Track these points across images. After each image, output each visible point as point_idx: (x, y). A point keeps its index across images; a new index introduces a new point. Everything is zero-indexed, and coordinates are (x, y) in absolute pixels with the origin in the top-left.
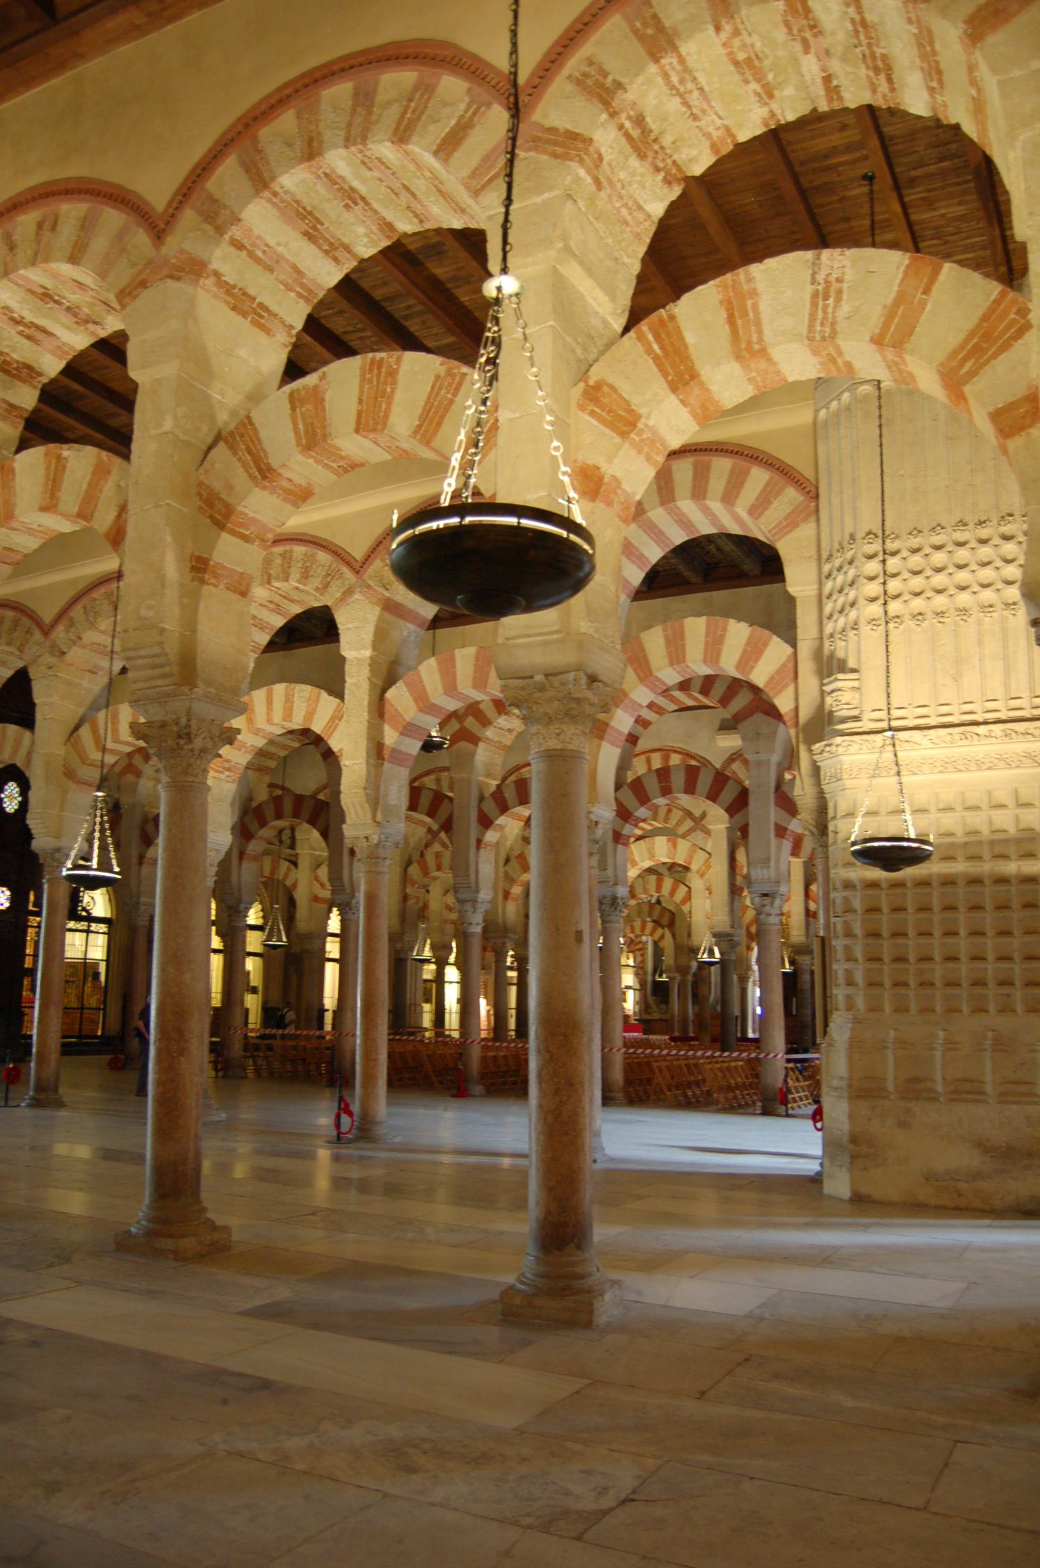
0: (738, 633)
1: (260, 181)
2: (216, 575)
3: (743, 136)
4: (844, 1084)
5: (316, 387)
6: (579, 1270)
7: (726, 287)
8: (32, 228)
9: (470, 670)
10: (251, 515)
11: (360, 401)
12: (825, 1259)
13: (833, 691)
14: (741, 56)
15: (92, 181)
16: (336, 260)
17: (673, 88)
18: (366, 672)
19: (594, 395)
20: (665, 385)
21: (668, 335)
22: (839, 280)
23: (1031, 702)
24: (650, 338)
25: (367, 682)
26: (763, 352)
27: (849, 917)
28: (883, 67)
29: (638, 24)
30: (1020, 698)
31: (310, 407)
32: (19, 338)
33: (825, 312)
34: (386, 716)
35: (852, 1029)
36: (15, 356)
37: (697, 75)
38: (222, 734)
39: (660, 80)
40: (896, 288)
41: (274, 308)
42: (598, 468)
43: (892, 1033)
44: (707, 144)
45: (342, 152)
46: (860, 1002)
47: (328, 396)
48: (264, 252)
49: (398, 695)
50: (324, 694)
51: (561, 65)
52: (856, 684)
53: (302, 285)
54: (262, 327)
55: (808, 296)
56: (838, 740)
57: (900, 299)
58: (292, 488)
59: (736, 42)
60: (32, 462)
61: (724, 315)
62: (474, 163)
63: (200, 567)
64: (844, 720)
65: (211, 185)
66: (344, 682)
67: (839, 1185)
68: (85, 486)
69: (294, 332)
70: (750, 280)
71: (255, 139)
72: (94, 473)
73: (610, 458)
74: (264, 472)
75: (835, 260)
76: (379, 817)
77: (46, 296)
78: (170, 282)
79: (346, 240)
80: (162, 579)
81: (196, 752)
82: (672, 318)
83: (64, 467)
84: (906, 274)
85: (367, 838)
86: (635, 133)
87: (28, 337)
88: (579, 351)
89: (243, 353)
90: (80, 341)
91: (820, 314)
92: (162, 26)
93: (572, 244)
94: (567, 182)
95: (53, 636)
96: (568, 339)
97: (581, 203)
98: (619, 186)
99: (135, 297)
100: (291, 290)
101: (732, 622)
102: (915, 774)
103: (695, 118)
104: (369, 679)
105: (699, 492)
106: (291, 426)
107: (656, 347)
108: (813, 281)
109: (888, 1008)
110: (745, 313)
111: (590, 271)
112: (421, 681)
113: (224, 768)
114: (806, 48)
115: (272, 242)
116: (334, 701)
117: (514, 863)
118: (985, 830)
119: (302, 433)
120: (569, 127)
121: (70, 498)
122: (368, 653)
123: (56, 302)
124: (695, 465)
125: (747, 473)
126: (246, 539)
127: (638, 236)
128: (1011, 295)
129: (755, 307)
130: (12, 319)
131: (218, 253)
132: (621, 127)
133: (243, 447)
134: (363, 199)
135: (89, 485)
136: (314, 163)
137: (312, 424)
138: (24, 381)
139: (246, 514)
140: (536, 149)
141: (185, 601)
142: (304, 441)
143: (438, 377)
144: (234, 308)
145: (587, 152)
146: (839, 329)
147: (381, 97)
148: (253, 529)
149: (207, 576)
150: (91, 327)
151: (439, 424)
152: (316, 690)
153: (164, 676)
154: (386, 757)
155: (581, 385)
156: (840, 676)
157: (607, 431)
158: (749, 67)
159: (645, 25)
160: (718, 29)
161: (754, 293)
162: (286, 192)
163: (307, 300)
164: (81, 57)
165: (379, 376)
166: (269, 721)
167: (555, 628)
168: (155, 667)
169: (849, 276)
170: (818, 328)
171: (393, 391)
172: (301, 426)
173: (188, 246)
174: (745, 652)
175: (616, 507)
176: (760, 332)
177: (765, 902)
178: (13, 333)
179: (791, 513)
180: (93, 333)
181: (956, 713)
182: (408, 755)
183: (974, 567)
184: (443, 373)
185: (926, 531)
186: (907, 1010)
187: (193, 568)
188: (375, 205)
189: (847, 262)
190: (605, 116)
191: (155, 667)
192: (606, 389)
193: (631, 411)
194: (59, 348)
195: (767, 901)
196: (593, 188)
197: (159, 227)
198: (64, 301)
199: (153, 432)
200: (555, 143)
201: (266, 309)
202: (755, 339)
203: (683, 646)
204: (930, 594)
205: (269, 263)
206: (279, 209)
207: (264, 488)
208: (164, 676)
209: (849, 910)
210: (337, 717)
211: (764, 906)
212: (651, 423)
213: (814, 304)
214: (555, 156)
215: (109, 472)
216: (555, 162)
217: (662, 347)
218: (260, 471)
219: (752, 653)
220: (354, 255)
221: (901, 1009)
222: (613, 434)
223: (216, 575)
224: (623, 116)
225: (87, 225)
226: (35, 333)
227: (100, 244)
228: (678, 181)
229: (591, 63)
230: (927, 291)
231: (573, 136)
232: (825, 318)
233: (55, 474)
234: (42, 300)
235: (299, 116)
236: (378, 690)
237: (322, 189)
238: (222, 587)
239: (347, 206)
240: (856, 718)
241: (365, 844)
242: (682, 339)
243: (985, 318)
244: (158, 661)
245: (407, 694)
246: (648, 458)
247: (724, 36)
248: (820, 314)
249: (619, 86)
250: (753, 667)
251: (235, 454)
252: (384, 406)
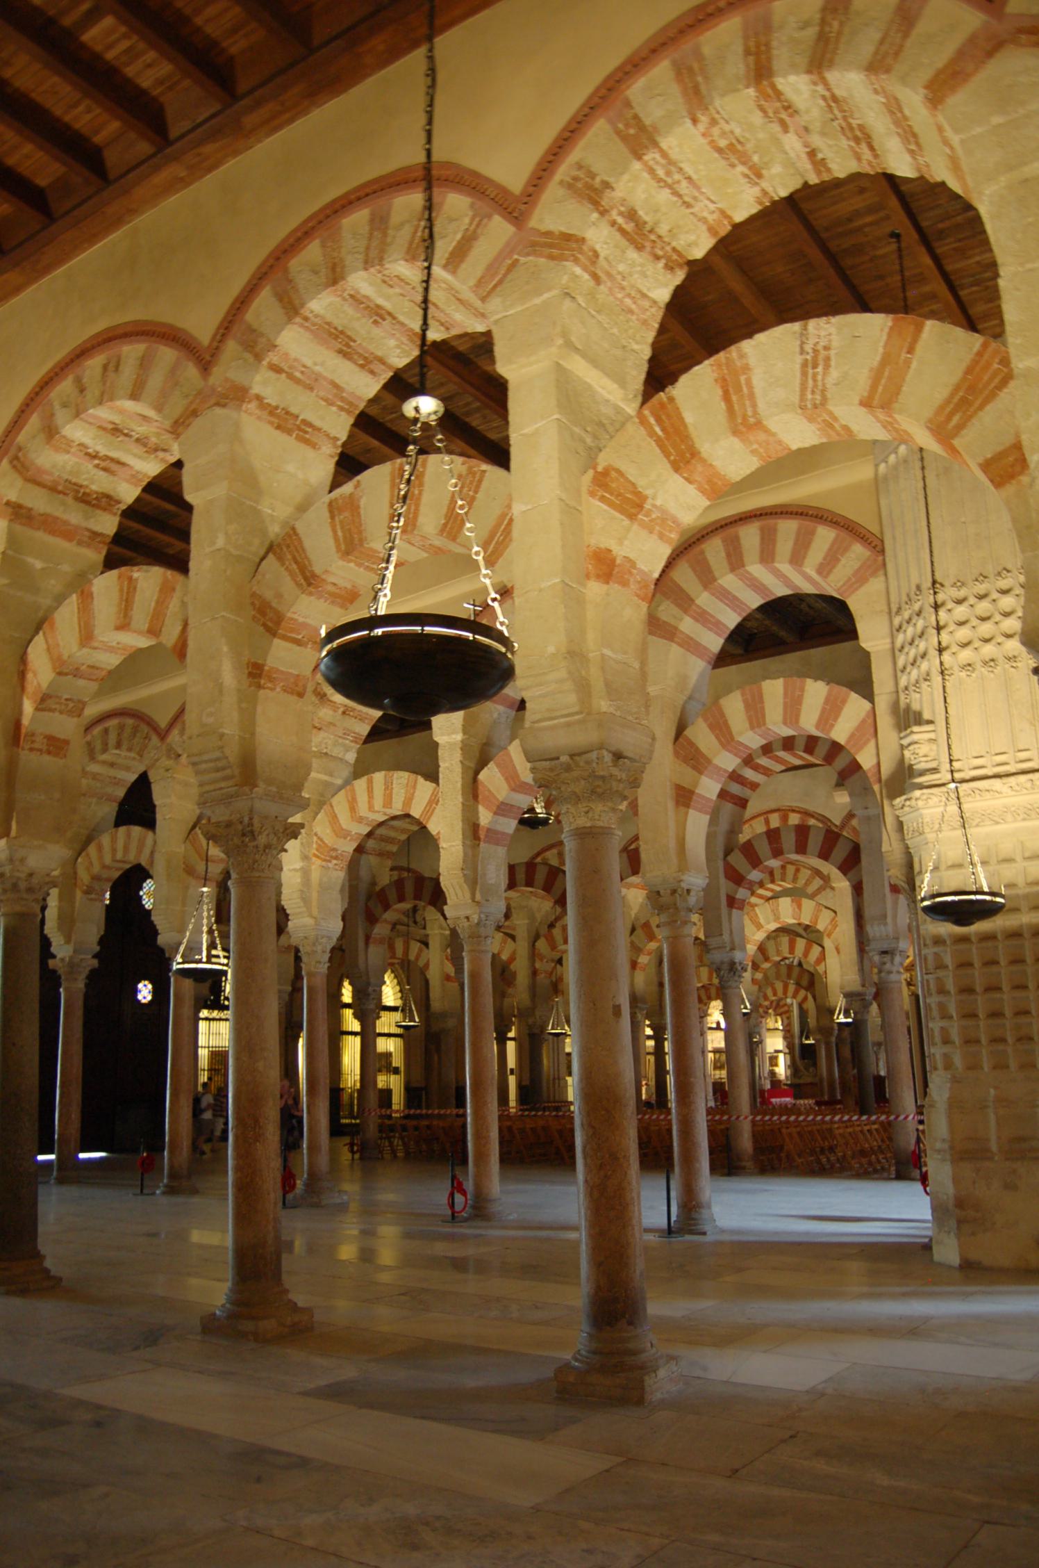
0: (816, 692)
1: (291, 308)
2: (271, 679)
3: (739, 217)
4: (946, 1146)
5: (351, 494)
6: (631, 1346)
7: (719, 365)
8: (99, 370)
10: (301, 620)
12: (913, 1330)
13: (909, 745)
14: (723, 143)
15: (146, 322)
16: (372, 372)
17: (660, 180)
18: (458, 755)
19: (604, 481)
20: (668, 466)
21: (669, 417)
22: (826, 348)
23: (1015, 756)
24: (652, 420)
25: (460, 765)
26: (759, 425)
27: (941, 973)
28: (862, 136)
29: (621, 126)
30: (982, 757)
31: (347, 514)
32: (95, 471)
33: (815, 380)
34: (480, 797)
35: (951, 1089)
36: (94, 487)
37: (682, 165)
38: (286, 829)
39: (645, 175)
40: (881, 350)
41: (318, 423)
42: (610, 551)
43: (992, 1091)
44: (704, 228)
45: (362, 274)
46: (958, 1061)
47: (363, 502)
48: (302, 372)
49: (490, 776)
50: (421, 780)
51: (552, 173)
52: (932, 736)
53: (343, 399)
54: (307, 442)
55: (798, 367)
56: (917, 793)
57: (886, 360)
58: (338, 591)
59: (715, 131)
60: (106, 585)
61: (720, 392)
62: (479, 271)
63: (256, 673)
64: (922, 773)
65: (249, 316)
66: (439, 766)
67: (948, 1252)
68: (153, 604)
69: (340, 443)
70: (742, 356)
71: (286, 271)
72: (161, 591)
73: (620, 542)
74: (309, 580)
75: (825, 330)
76: (478, 897)
77: (116, 430)
78: (218, 410)
79: (379, 353)
80: (220, 688)
81: (261, 849)
82: (671, 399)
83: (135, 588)
84: (890, 336)
85: (467, 918)
86: (629, 227)
87: (105, 469)
88: (589, 440)
89: (291, 468)
90: (151, 468)
91: (810, 382)
92: (202, 177)
93: (573, 339)
94: (564, 282)
95: (169, 739)
96: (577, 430)
97: (580, 300)
98: (619, 277)
99: (188, 426)
100: (332, 404)
101: (809, 682)
102: (997, 823)
103: (688, 205)
104: (461, 762)
105: (767, 556)
106: (331, 534)
107: (657, 429)
108: (802, 351)
109: (986, 1067)
110: (739, 389)
111: (594, 362)
112: (512, 761)
113: (332, 857)
114: (785, 127)
115: (309, 363)
116: (430, 786)
117: (639, 932)
118: (1020, 881)
119: (341, 539)
120: (563, 229)
121: (141, 615)
122: (459, 737)
123: (126, 435)
124: (762, 530)
125: (813, 533)
126: (298, 642)
127: (645, 323)
128: (994, 345)
129: (749, 382)
130: (87, 454)
131: (258, 378)
132: (613, 223)
133: (289, 557)
134: (390, 314)
135: (157, 602)
136: (338, 286)
137: (350, 530)
138: (105, 510)
139: (296, 620)
140: (534, 253)
141: (244, 705)
142: (343, 547)
144: (278, 427)
145: (581, 251)
146: (829, 396)
147: (395, 219)
148: (304, 633)
149: (262, 682)
150: (161, 454)
152: (413, 776)
153: (225, 779)
154: (482, 837)
155: (591, 473)
156: (915, 729)
157: (617, 515)
158: (733, 152)
159: (627, 126)
160: (695, 121)
161: (746, 369)
162: (316, 316)
163: (349, 412)
164: (133, 212)
166: (371, 808)
167: (576, 709)
168: (218, 770)
169: (835, 343)
170: (809, 396)
172: (340, 533)
173: (231, 375)
174: (824, 710)
175: (633, 586)
176: (754, 406)
178: (90, 466)
180: (163, 460)
182: (504, 834)
184: (464, 473)
185: (991, 576)
186: (1008, 1067)
187: (250, 675)
188: (401, 318)
189: (833, 330)
190: (595, 215)
191: (218, 770)
192: (613, 474)
193: (638, 494)
194: (133, 476)
195: (887, 958)
196: (592, 283)
197: (205, 360)
198: (133, 433)
199: (208, 550)
200: (551, 246)
201: (310, 425)
202: (750, 413)
203: (763, 709)
204: (1000, 639)
205: (308, 382)
206: (312, 331)
207: (311, 594)
208: (225, 779)
209: (941, 966)
210: (434, 801)
211: (885, 963)
212: (658, 503)
213: (804, 374)
214: (551, 257)
215: (174, 590)
216: (552, 264)
217: (663, 430)
218: (306, 579)
219: (831, 711)
220: (390, 367)
221: (1000, 1066)
222: (623, 517)
223: (271, 679)
224: (614, 213)
225: (145, 363)
226: (110, 465)
227: (156, 380)
228: (680, 266)
229: (580, 166)
230: (911, 351)
231: (567, 237)
232: (815, 386)
233: (128, 593)
234: (113, 435)
235: (323, 246)
236: (471, 773)
237: (350, 310)
238: (278, 689)
239: (375, 322)
240: (935, 770)
241: (466, 924)
242: (681, 419)
243: (969, 371)
244: (220, 764)
245: (499, 775)
246: (661, 536)
247: (702, 127)
248: (810, 382)
249: (607, 185)
250: (833, 726)
251: (283, 564)
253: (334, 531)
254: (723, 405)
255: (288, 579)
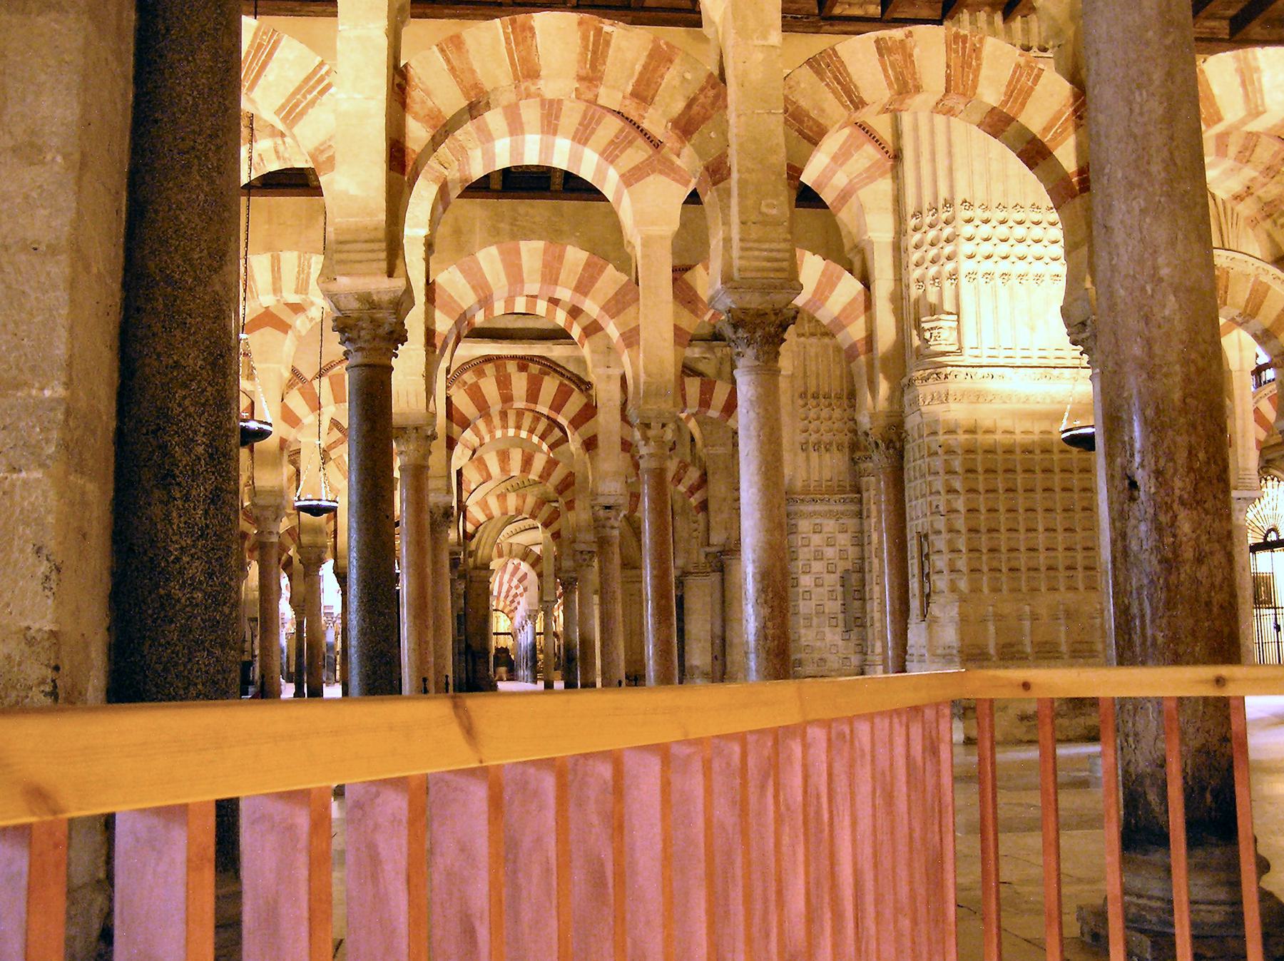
9: (538, 264)
11: (948, 66)
35: (960, 607)
43: (991, 608)
46: (963, 585)
47: (916, 52)
70: (1255, 59)
72: (651, 56)
102: (1005, 402)
109: (986, 590)
110: (1252, 83)
129: (1260, 82)
135: (645, 67)
137: (902, 73)
143: (1018, 66)
151: (1023, 105)
161: (1257, 70)
165: (964, 48)
168: (769, 260)
171: (979, 66)
172: (890, 72)
177: (609, 515)
179: (869, 167)
181: (1035, 358)
183: (1047, 244)
185: (1010, 207)
191: (769, 260)
199: (757, 42)
202: (1259, 102)
215: (671, 61)
221: (996, 590)
251: (822, 79)
252: (971, 77)
253: (885, 70)
254: (1241, 90)
255: (831, 96)
